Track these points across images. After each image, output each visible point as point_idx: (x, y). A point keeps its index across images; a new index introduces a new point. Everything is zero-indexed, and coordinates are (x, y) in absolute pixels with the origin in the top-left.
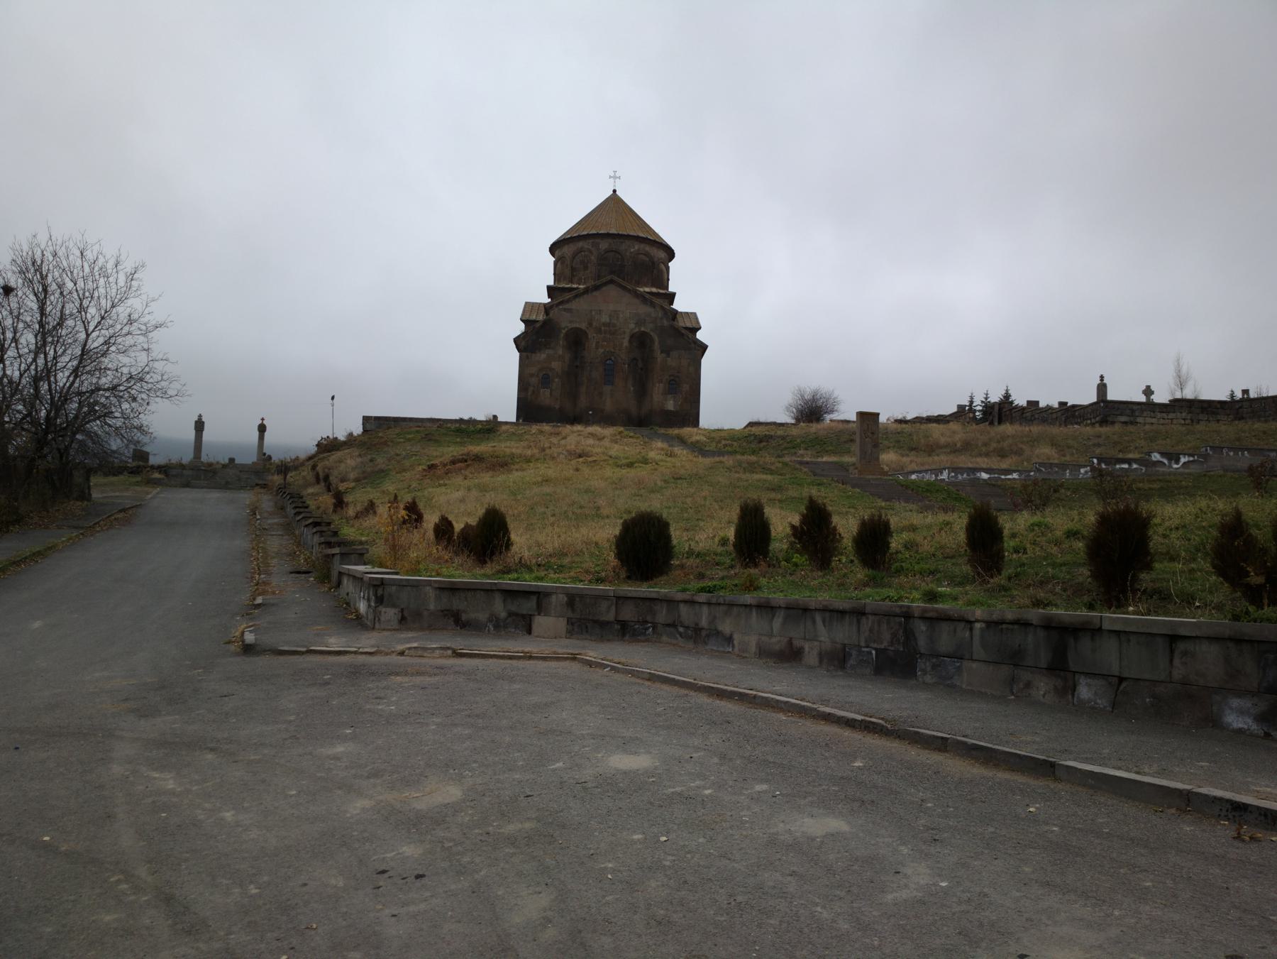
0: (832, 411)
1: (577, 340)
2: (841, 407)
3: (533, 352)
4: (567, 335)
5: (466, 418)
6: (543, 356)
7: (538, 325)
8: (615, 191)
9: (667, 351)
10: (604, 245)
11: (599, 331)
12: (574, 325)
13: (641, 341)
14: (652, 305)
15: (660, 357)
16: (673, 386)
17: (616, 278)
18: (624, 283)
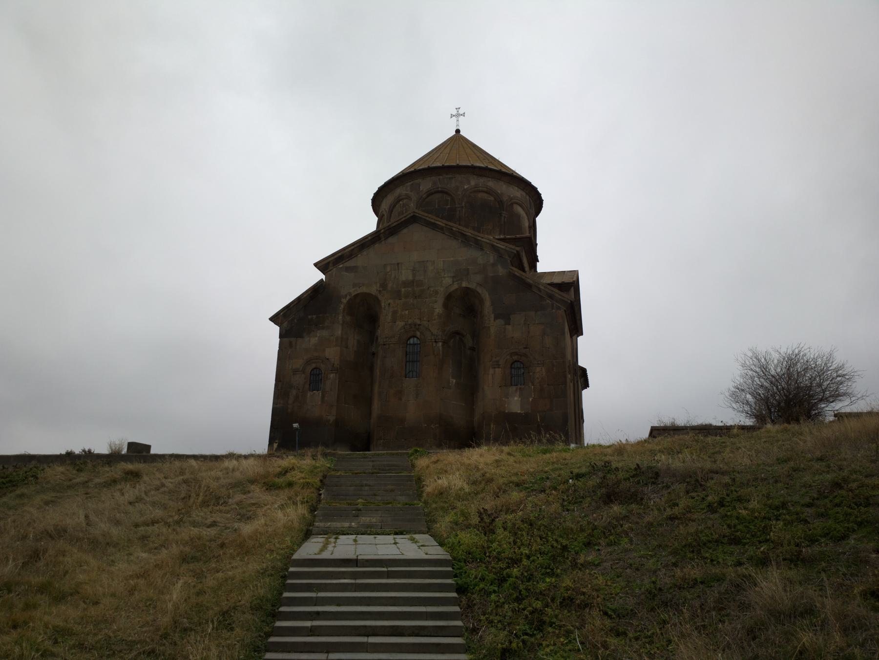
0: (837, 396)
1: (366, 314)
2: (858, 386)
3: (299, 335)
5: (77, 451)
6: (314, 340)
8: (458, 131)
9: (505, 315)
10: (426, 185)
11: (397, 295)
12: (364, 290)
13: (464, 304)
14: (479, 245)
15: (493, 325)
16: (518, 370)
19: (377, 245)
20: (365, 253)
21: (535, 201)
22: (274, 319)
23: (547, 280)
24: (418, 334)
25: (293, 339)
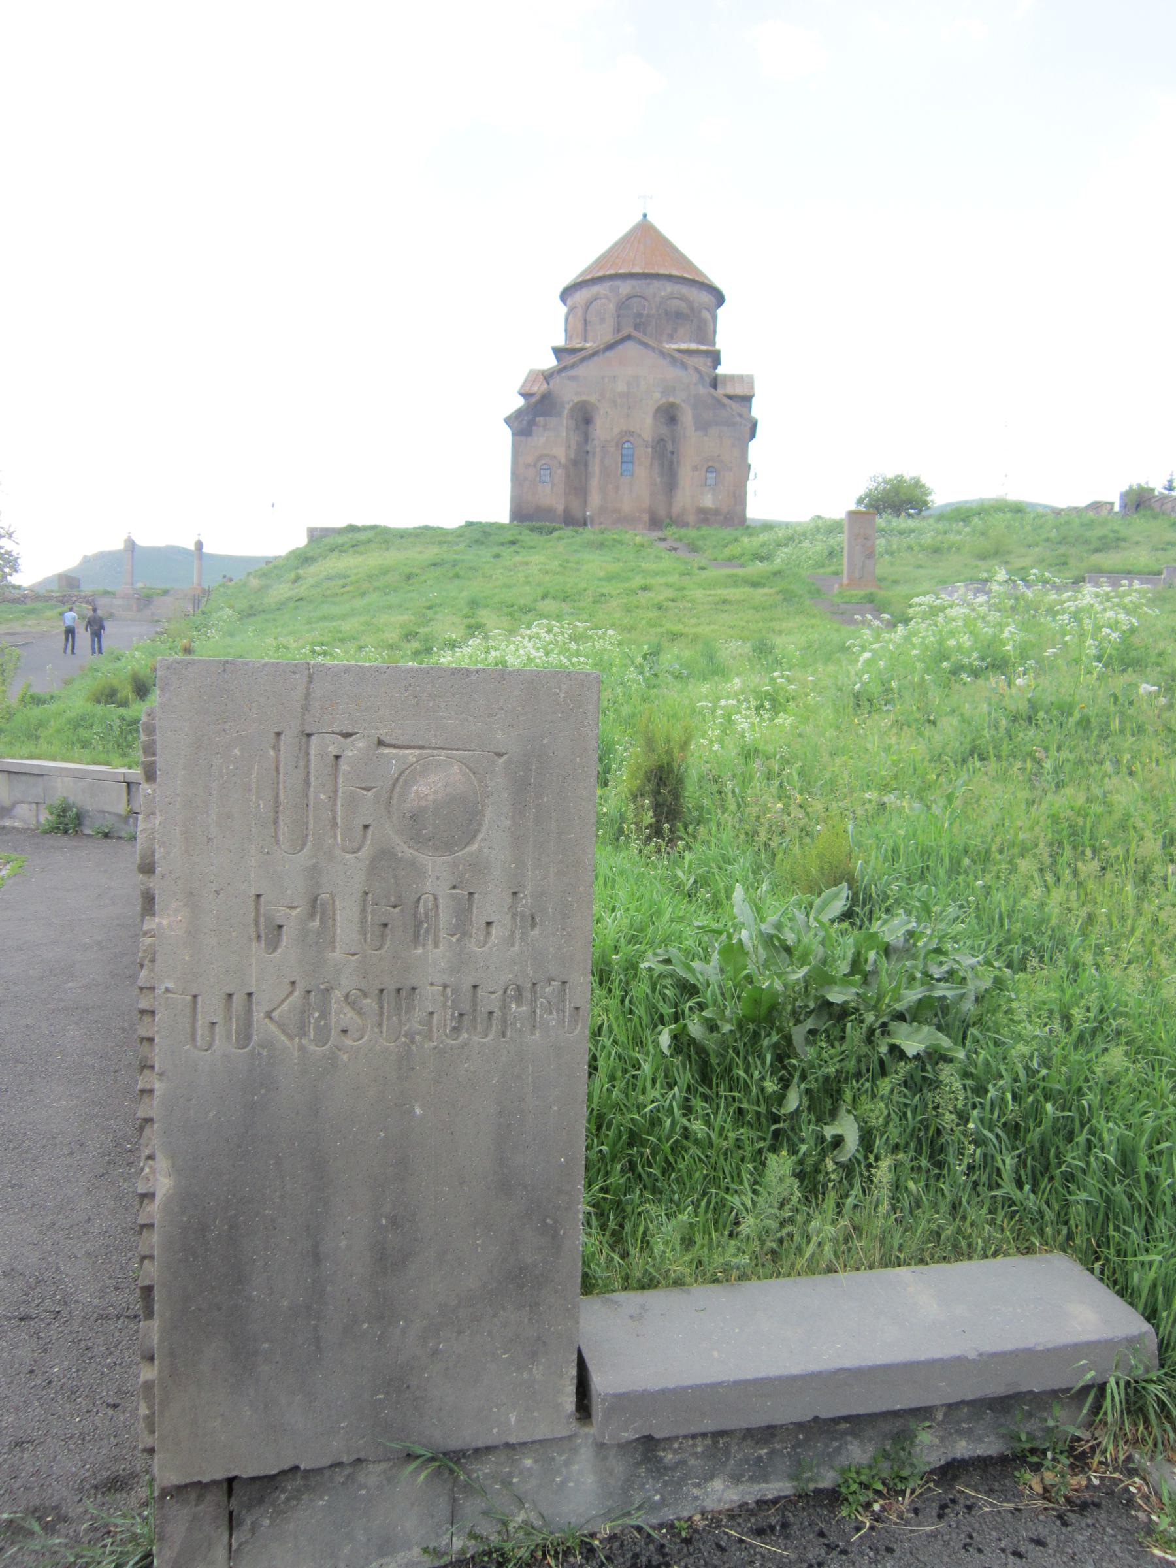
4: (572, 410)
6: (542, 440)
7: (534, 400)
8: (645, 216)
10: (625, 288)
12: (584, 398)
13: (669, 415)
14: (684, 366)
17: (634, 333)
18: (646, 339)
19: (596, 358)
20: (585, 364)
21: (720, 299)
22: (508, 421)
23: (730, 391)
24: (632, 439)
25: (523, 438)
